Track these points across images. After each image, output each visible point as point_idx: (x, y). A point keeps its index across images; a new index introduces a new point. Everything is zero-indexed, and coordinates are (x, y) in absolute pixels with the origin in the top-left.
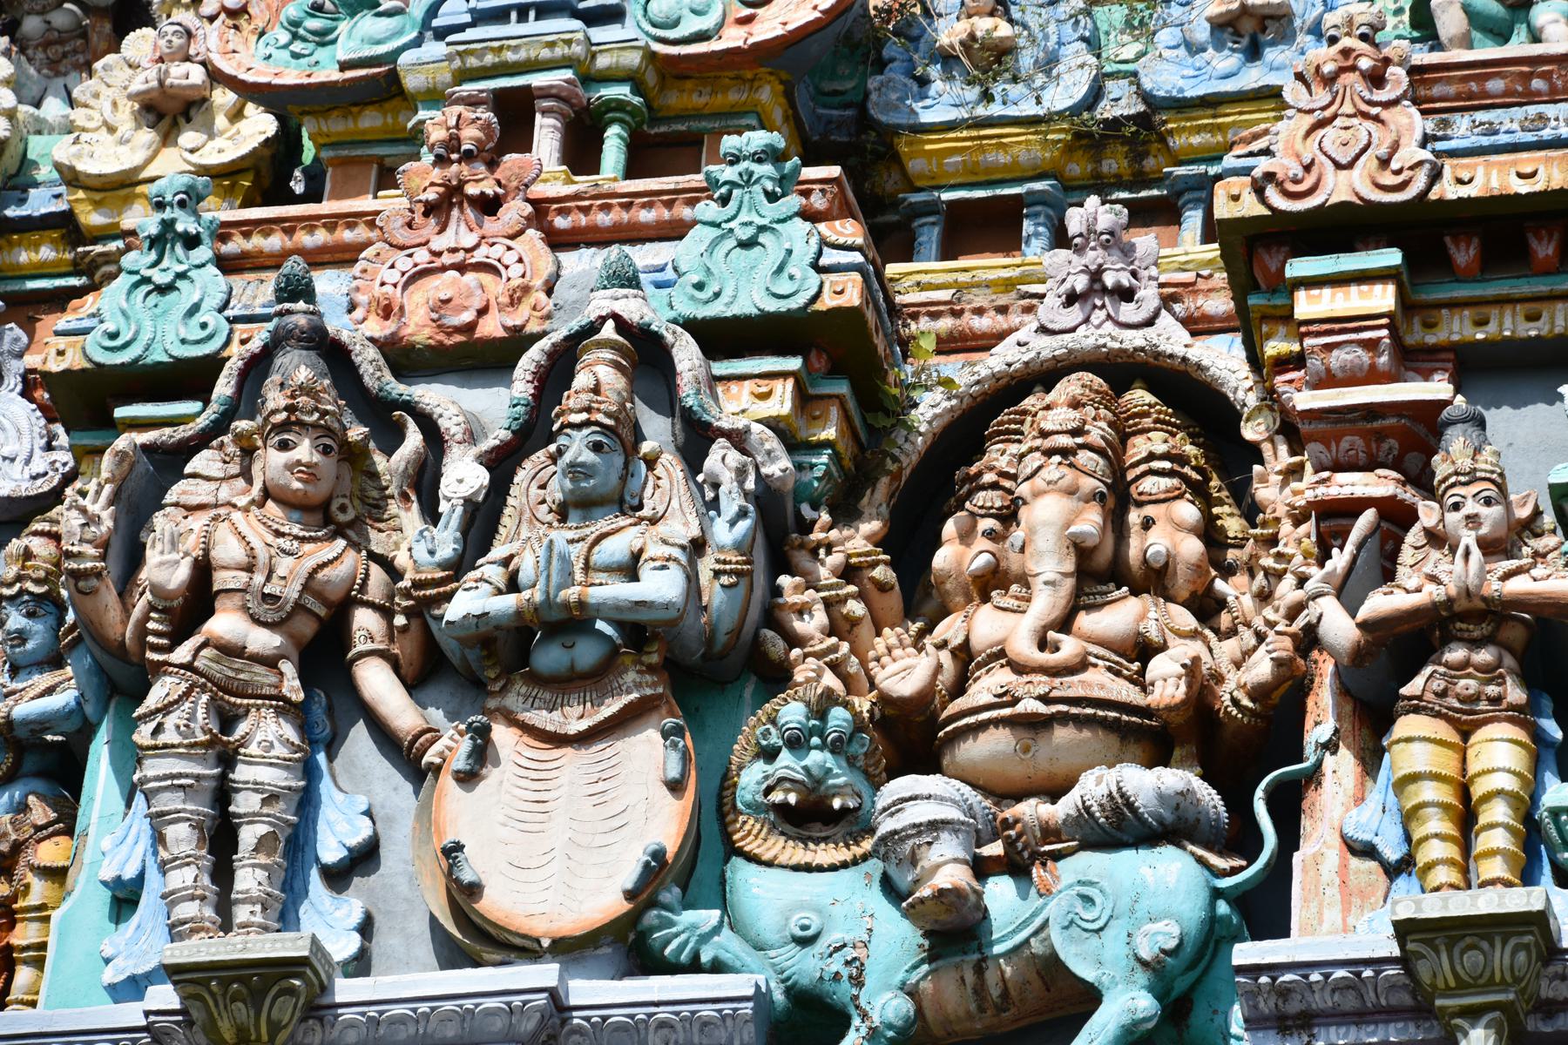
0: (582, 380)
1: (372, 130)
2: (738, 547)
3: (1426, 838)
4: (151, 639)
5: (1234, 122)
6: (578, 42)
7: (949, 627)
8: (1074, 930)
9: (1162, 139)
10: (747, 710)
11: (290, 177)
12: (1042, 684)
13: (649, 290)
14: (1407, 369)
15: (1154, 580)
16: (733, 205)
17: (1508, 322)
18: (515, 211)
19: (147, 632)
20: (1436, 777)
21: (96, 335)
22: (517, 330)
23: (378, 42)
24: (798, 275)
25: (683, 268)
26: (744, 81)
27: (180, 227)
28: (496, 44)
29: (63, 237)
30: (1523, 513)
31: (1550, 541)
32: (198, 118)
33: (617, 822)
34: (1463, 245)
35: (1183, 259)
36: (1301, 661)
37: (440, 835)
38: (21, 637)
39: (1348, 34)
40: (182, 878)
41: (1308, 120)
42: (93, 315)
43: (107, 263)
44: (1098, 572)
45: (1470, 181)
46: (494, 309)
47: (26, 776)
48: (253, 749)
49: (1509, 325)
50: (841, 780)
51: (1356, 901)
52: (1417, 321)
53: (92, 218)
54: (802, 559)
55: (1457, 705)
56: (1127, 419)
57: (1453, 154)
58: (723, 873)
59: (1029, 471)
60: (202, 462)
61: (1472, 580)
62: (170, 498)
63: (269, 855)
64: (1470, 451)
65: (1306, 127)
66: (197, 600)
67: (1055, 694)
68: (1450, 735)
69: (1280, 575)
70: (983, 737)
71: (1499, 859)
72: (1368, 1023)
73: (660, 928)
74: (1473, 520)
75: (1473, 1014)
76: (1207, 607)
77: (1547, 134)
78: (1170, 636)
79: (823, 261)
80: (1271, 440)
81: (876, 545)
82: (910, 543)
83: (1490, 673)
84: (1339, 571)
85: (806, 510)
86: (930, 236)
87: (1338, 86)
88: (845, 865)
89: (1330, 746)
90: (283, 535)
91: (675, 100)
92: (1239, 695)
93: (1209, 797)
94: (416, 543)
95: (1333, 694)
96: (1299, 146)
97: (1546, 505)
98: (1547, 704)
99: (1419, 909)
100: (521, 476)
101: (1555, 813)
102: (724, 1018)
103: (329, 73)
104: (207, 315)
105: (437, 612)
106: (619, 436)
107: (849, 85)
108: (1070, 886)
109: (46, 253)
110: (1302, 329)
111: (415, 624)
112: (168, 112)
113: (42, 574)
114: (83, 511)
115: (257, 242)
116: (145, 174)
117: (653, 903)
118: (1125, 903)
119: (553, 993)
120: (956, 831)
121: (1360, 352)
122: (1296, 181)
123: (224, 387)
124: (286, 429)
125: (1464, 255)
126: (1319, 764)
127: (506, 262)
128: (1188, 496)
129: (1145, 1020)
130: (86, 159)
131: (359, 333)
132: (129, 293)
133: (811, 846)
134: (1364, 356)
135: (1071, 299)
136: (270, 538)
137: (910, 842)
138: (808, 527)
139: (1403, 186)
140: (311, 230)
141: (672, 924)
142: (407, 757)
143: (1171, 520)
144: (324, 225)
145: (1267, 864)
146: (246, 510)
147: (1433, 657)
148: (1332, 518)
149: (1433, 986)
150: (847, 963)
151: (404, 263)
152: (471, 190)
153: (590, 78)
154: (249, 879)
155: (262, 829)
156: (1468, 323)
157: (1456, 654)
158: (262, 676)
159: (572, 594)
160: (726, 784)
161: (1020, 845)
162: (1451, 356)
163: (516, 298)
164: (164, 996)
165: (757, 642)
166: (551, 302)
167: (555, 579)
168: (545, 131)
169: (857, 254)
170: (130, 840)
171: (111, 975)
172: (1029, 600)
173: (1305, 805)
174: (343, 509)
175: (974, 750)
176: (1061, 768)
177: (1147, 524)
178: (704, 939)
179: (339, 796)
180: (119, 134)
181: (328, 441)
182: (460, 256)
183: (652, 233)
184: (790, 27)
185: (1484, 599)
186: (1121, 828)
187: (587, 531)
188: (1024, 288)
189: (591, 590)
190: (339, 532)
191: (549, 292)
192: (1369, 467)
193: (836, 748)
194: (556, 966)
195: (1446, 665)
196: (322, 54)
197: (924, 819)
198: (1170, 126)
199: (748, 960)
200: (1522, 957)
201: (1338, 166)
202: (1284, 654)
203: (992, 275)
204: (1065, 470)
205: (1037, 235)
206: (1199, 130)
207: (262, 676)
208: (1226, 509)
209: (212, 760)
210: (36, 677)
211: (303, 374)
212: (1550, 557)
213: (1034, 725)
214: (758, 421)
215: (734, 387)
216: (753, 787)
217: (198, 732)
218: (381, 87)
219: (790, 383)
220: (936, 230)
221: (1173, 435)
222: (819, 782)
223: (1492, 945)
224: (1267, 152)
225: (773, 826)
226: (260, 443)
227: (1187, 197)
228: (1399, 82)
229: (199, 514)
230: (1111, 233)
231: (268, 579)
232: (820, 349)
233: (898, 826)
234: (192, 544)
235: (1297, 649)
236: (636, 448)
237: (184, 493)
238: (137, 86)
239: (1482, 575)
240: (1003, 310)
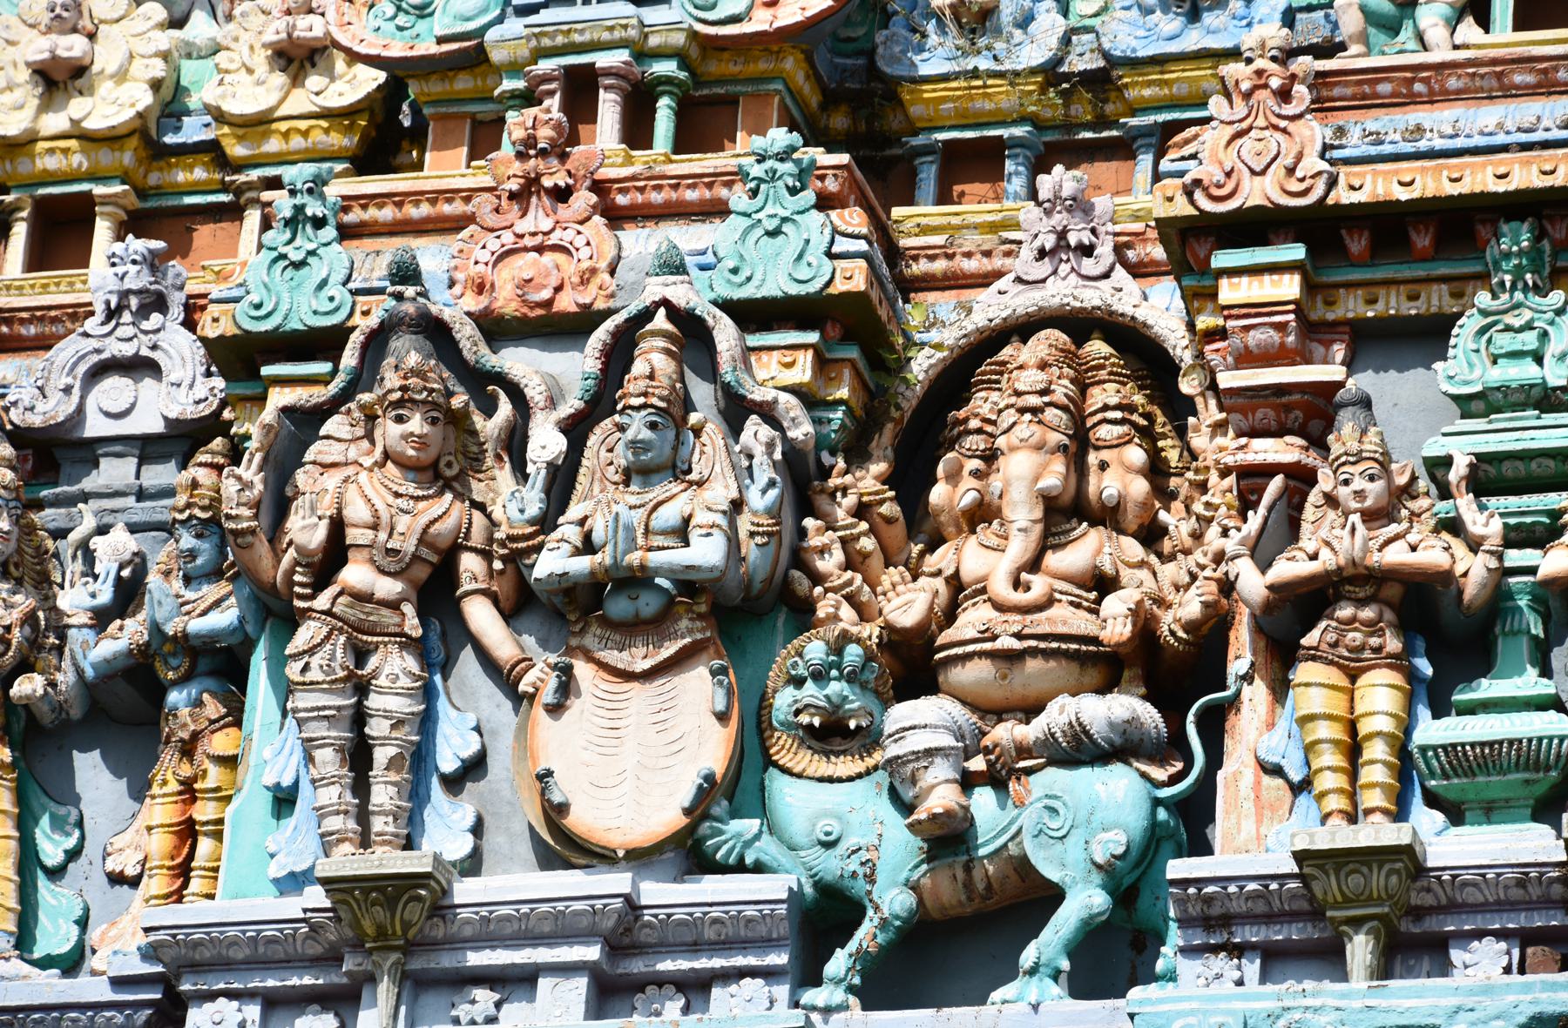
0: (639, 367)
1: (465, 91)
2: (769, 512)
3: (1321, 770)
4: (297, 589)
5: (1178, 79)
6: (633, 27)
7: (943, 557)
8: (1043, 838)
9: (1119, 89)
10: (780, 639)
11: (399, 110)
12: (1015, 622)
13: (694, 272)
14: (1312, 340)
15: (1108, 516)
16: (761, 197)
17: (1393, 302)
18: (583, 199)
19: (293, 584)
20: (1329, 717)
21: (244, 304)
22: (586, 307)
23: (468, 19)
24: (815, 263)
25: (721, 254)
26: (772, 53)
27: (309, 212)
28: (565, 27)
29: (212, 160)
30: (1402, 480)
31: (1424, 503)
32: (321, 63)
33: (676, 747)
34: (1356, 237)
35: (1135, 207)
36: (1224, 601)
37: (534, 760)
38: (192, 554)
39: (1261, 56)
40: (328, 795)
41: (1229, 131)
42: (241, 285)
43: (250, 189)
44: (1065, 512)
46: (567, 287)
47: (200, 675)
48: (382, 681)
49: (1394, 304)
50: (855, 705)
51: (1267, 813)
52: (1319, 299)
53: (236, 150)
54: (822, 502)
56: (1087, 371)
57: (1347, 162)
58: (763, 781)
59: (1005, 426)
60: (333, 425)
61: (1357, 553)
62: (308, 457)
63: (398, 772)
64: (1357, 435)
65: (1227, 138)
66: (335, 552)
67: (1027, 631)
68: (1343, 681)
69: (1210, 520)
70: (969, 665)
71: (1378, 790)
72: (1275, 923)
73: (712, 837)
74: (1360, 495)
75: (1357, 923)
76: (1152, 535)
77: (1423, 145)
78: (1121, 567)
79: (835, 249)
80: (1202, 394)
81: (884, 483)
82: (911, 480)
83: (1373, 627)
84: (1253, 533)
85: (826, 458)
86: (928, 175)
87: (1253, 101)
88: (860, 776)
89: (1247, 678)
90: (401, 496)
91: (715, 68)
92: (1174, 627)
93: (1150, 715)
94: (511, 500)
95: (1250, 631)
96: (1221, 155)
97: (1421, 472)
98: (1421, 645)
99: (1312, 842)
100: (593, 440)
101: (1423, 749)
102: (764, 916)
103: (428, 47)
104: (335, 289)
105: (527, 562)
106: (671, 415)
107: (861, 32)
108: (1040, 799)
109: (199, 174)
110: (1227, 310)
111: (510, 567)
112: (298, 59)
113: (207, 502)
114: (239, 478)
115: (373, 213)
116: (279, 113)
117: (706, 816)
118: (1082, 815)
119: (627, 898)
120: (947, 756)
121: (1272, 332)
122: (1219, 186)
123: (349, 358)
124: (402, 405)
125: (1357, 245)
126: (1238, 693)
127: (577, 244)
128: (1136, 440)
129: (1099, 914)
130: (229, 99)
131: (455, 308)
132: (270, 267)
133: (833, 758)
134: (1275, 336)
135: (1042, 254)
136: (390, 499)
137: (911, 766)
138: (826, 473)
140: (417, 203)
141: (721, 833)
142: (505, 678)
143: (1122, 463)
144: (428, 200)
145: (1197, 780)
146: (371, 470)
147: (1328, 611)
148: (1251, 478)
149: (1325, 900)
150: (862, 864)
151: (494, 244)
152: (547, 182)
153: (643, 55)
154: (383, 795)
155: (392, 751)
156: (1360, 301)
157: (1345, 611)
158: (388, 617)
159: (635, 558)
160: (763, 704)
161: (998, 766)
162: (1347, 329)
163: (586, 278)
164: (316, 897)
165: (787, 582)
166: (614, 282)
167: (621, 546)
168: (607, 105)
169: (863, 242)
170: (286, 751)
171: (277, 869)
172: (1006, 539)
173: (1228, 726)
174: (449, 465)
175: (961, 675)
176: (1034, 691)
177: (1103, 466)
178: (748, 844)
179: (453, 713)
180: (256, 76)
181: (435, 414)
182: (539, 238)
183: (696, 209)
184: (809, 13)
185: (1367, 568)
186: (1079, 750)
187: (651, 496)
188: (1005, 235)
189: (650, 554)
190: (447, 485)
191: (612, 273)
192: (1278, 434)
193: (851, 678)
194: (629, 875)
195: (1338, 620)
196: (422, 26)
197: (921, 747)
198: (1126, 80)
199: (783, 860)
200: (1394, 879)
201: (1253, 172)
202: (1210, 598)
203: (979, 219)
204: (1035, 427)
205: (1017, 173)
206: (1149, 84)
207: (388, 617)
208: (1169, 442)
209: (349, 690)
210: (205, 588)
211: (413, 359)
213: (1010, 658)
214: (785, 389)
215: (765, 356)
216: (785, 709)
217: (338, 669)
218: (470, 56)
219: (810, 353)
220: (934, 168)
221: (1125, 384)
222: (838, 707)
223: (1371, 870)
224: (1193, 156)
225: (802, 742)
226: (380, 412)
227: (1140, 142)
229: (332, 471)
230: (1074, 199)
231: (390, 535)
232: (835, 320)
233: (901, 753)
234: (327, 508)
235: (1221, 591)
236: (685, 419)
237: (320, 452)
238: (270, 37)
239: (1366, 550)
240: (987, 254)
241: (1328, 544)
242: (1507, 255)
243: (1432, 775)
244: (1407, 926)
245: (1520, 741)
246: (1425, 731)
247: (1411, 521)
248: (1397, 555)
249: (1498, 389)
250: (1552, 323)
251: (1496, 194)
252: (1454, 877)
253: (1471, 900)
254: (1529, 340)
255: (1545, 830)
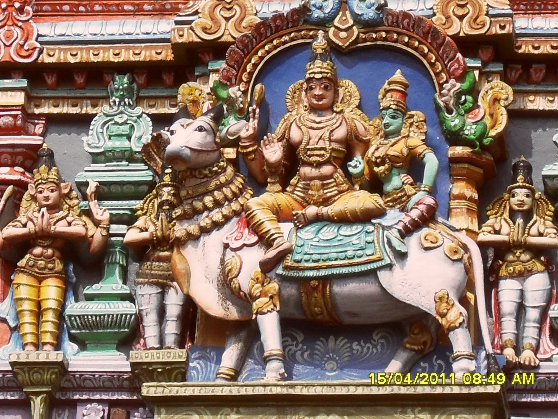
3: (24, 323)
30: (66, 191)
34: (50, 77)
45: (53, 55)
52: (32, 104)
55: (37, 271)
64: (47, 171)
71: (49, 334)
74: (47, 198)
75: (37, 394)
83: (49, 259)
97: (74, 187)
99: (18, 358)
101: (70, 316)
125: (50, 80)
139: (29, 56)
147: (29, 251)
149: (23, 383)
157: (38, 250)
192: (12, 165)
212: (75, 208)
228: (28, 14)
239: (49, 224)
241: (32, 220)
242: (117, 90)
243: (73, 328)
244: (58, 396)
245: (113, 315)
246: (72, 307)
247: (69, 211)
248: (61, 227)
249: (110, 151)
250: (136, 122)
251: (114, 62)
252: (81, 376)
253: (88, 386)
254: (125, 129)
255: (123, 355)
